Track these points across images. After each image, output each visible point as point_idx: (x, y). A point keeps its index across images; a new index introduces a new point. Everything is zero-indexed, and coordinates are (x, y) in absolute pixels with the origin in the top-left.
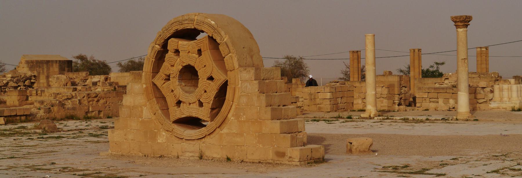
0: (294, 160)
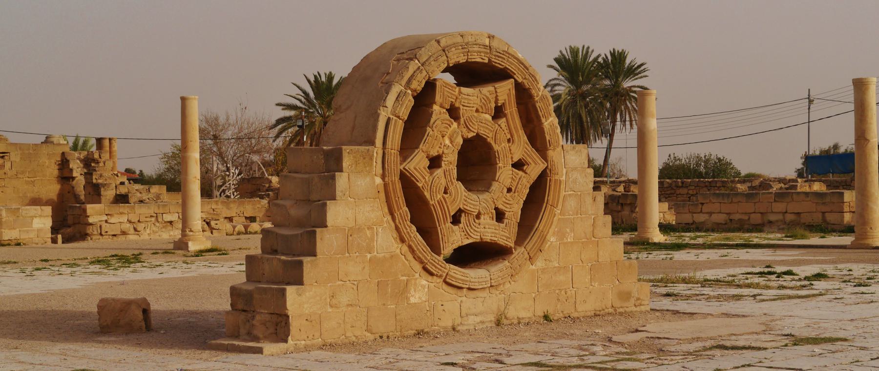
0: (643, 303)
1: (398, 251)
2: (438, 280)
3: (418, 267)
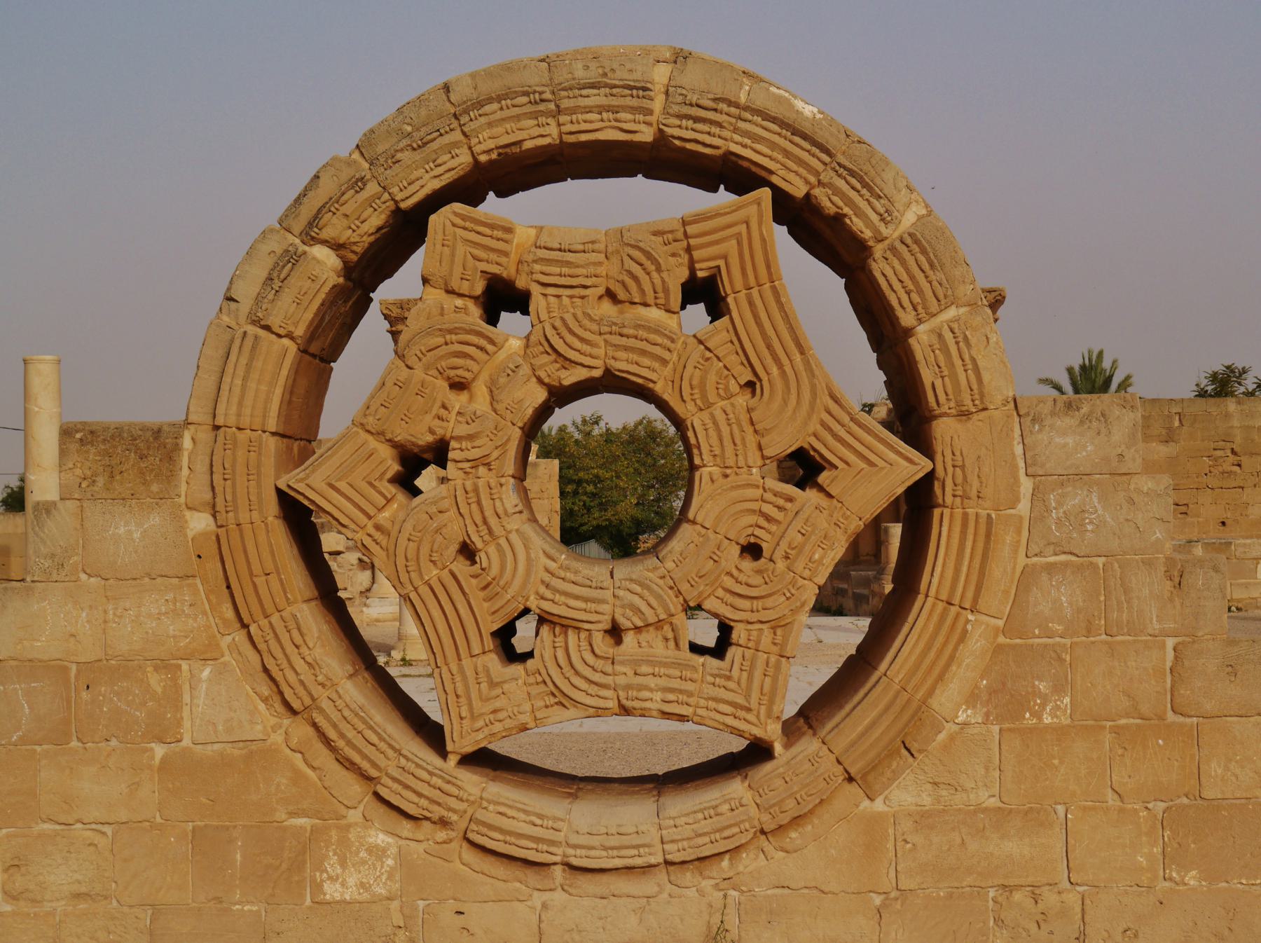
1: (278, 738)
2: (442, 835)
3: (353, 788)
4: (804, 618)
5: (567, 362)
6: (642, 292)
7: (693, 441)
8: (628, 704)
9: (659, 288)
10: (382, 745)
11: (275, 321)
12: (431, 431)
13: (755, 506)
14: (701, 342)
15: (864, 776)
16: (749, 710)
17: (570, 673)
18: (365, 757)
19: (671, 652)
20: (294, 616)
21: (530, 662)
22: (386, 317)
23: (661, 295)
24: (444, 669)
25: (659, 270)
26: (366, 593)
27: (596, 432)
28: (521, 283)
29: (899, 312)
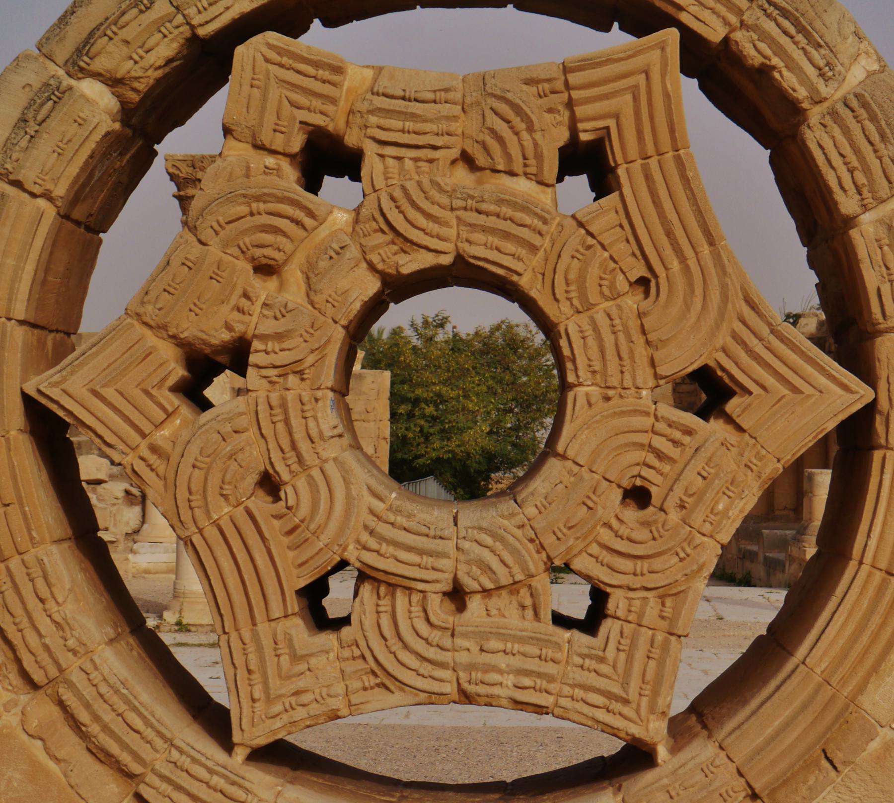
1: (12, 719)
4: (701, 585)
5: (408, 244)
6: (508, 157)
7: (566, 352)
8: (471, 688)
9: (530, 153)
10: (149, 733)
11: (28, 176)
12: (229, 327)
13: (643, 439)
14: (581, 225)
15: (773, 791)
16: (626, 702)
17: (396, 646)
18: (125, 747)
19: (529, 624)
20: (40, 562)
21: (345, 631)
22: (173, 177)
23: (532, 162)
24: (234, 637)
25: (530, 129)
26: (134, 535)
27: (441, 337)
28: (352, 139)
29: (839, 196)
